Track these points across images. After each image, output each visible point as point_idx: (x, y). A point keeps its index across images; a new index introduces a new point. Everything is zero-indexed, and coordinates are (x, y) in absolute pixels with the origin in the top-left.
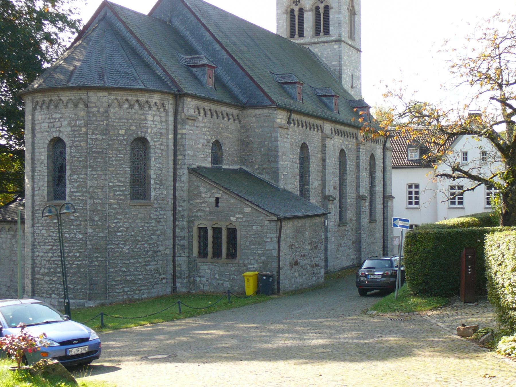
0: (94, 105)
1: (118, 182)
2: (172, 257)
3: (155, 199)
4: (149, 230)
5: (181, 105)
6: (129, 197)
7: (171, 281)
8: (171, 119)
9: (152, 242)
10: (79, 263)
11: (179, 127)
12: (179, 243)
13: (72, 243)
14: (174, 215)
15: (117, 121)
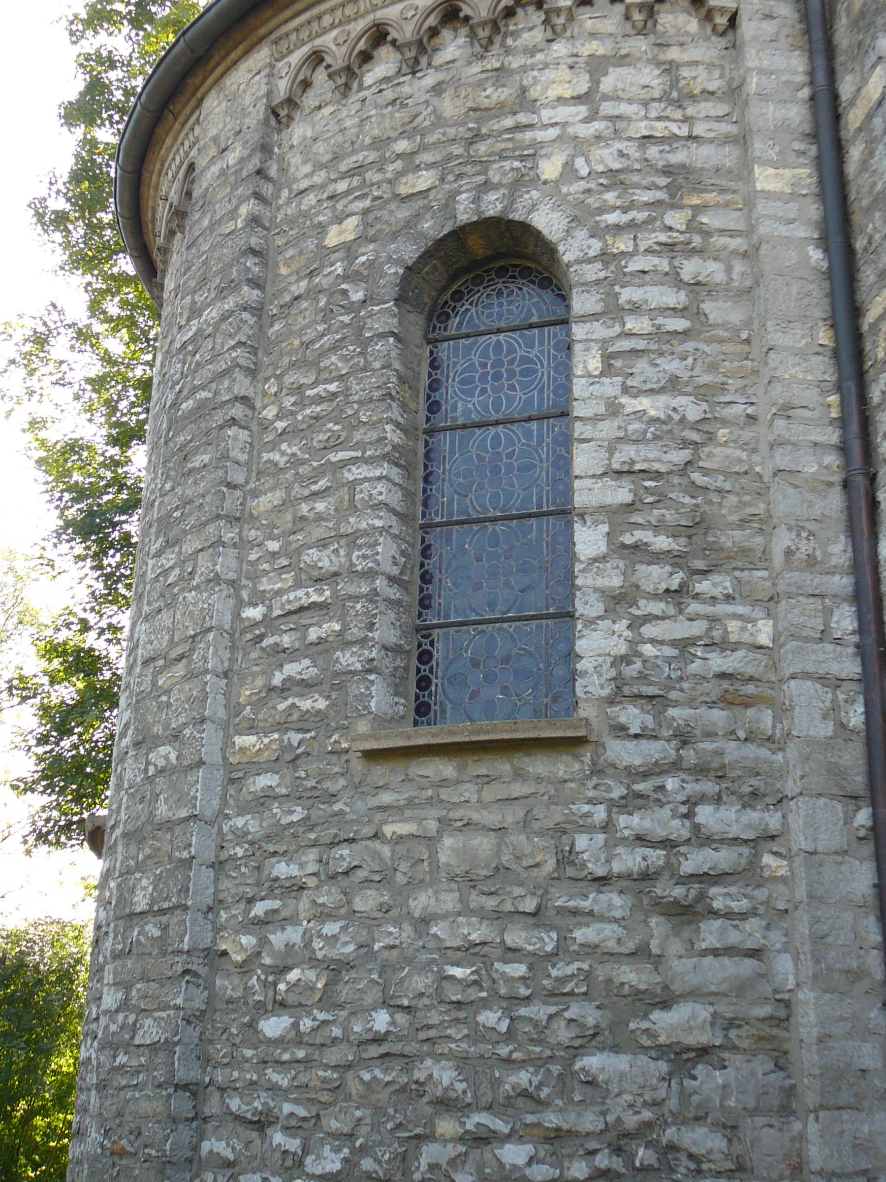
3: (620, 693)
9: (590, 1122)
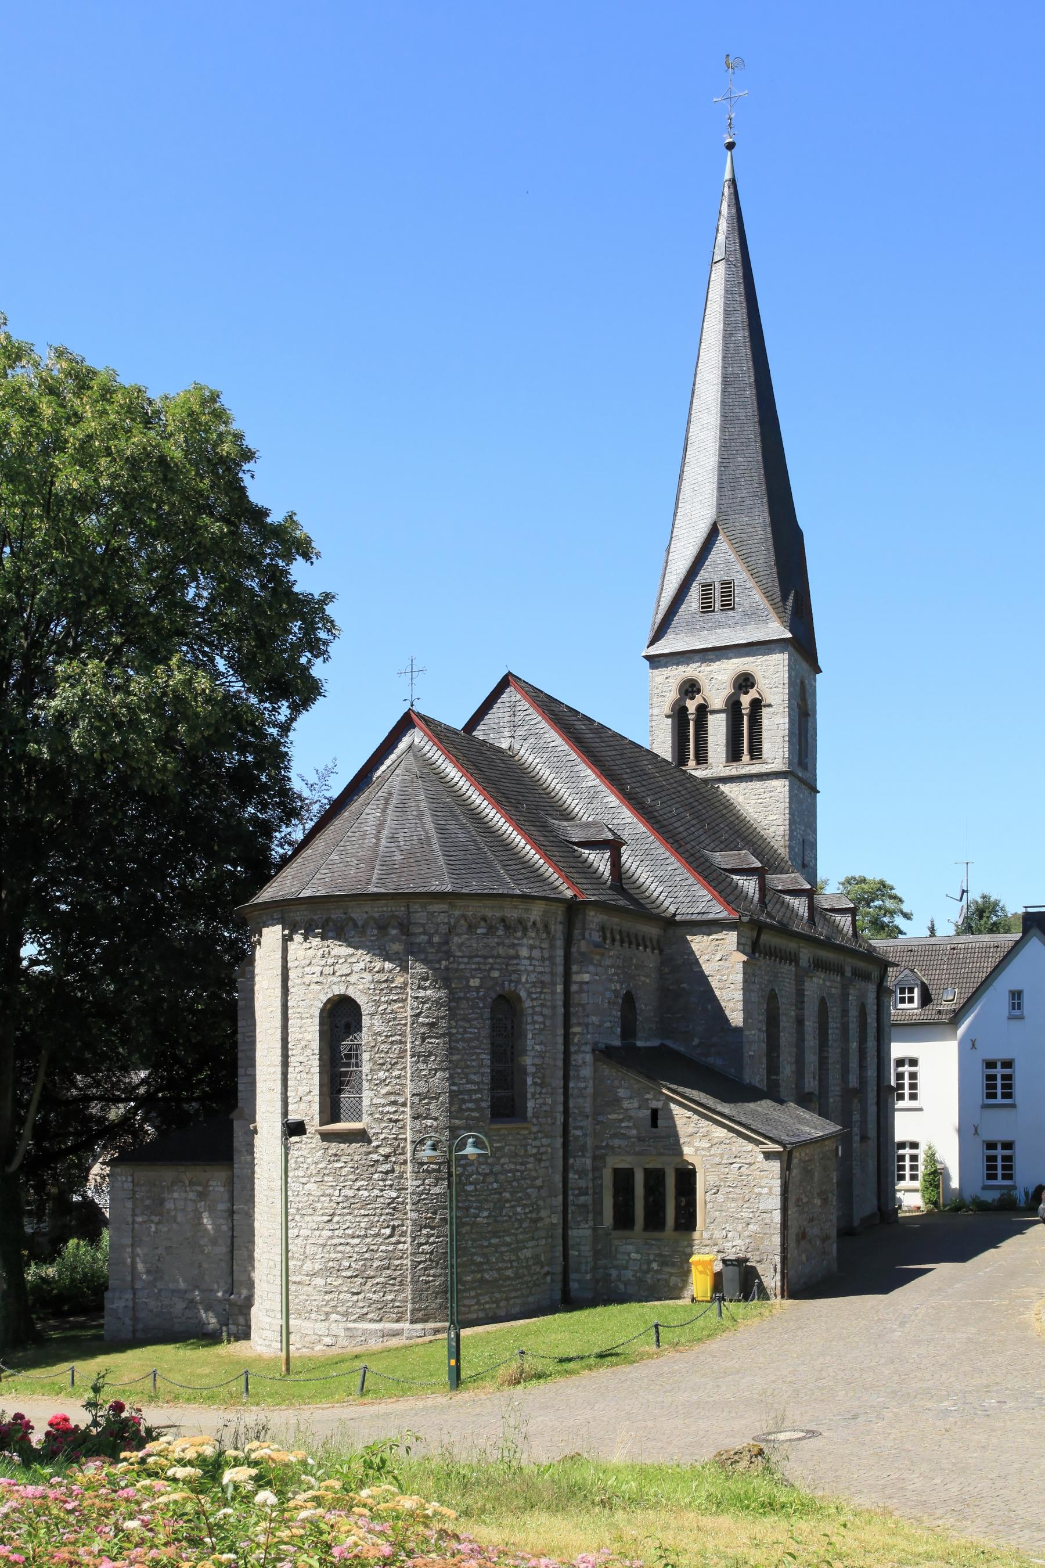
0: (421, 930)
1: (467, 1083)
2: (560, 1231)
3: (534, 1116)
4: (525, 1179)
5: (578, 925)
6: (488, 1112)
7: (560, 1277)
8: (560, 952)
10: (391, 1248)
11: (575, 968)
12: (576, 1202)
13: (375, 1209)
14: (565, 1145)
15: (466, 960)
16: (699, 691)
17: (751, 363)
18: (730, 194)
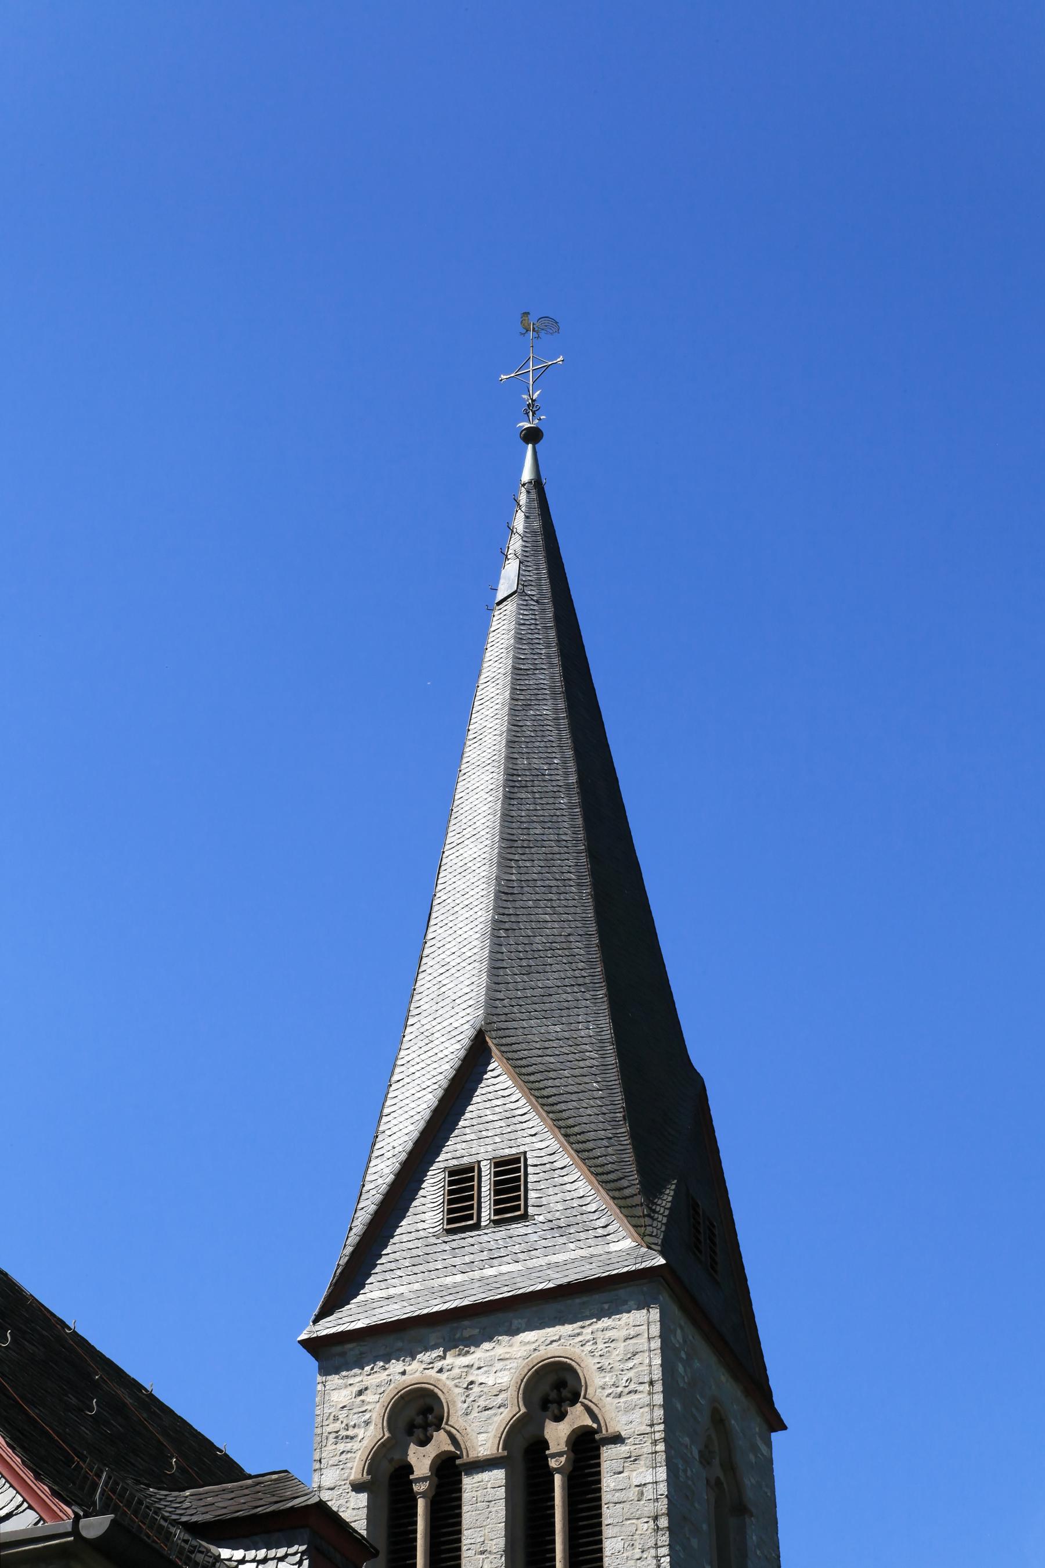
16: (438, 1424)
17: (570, 753)
18: (530, 501)
